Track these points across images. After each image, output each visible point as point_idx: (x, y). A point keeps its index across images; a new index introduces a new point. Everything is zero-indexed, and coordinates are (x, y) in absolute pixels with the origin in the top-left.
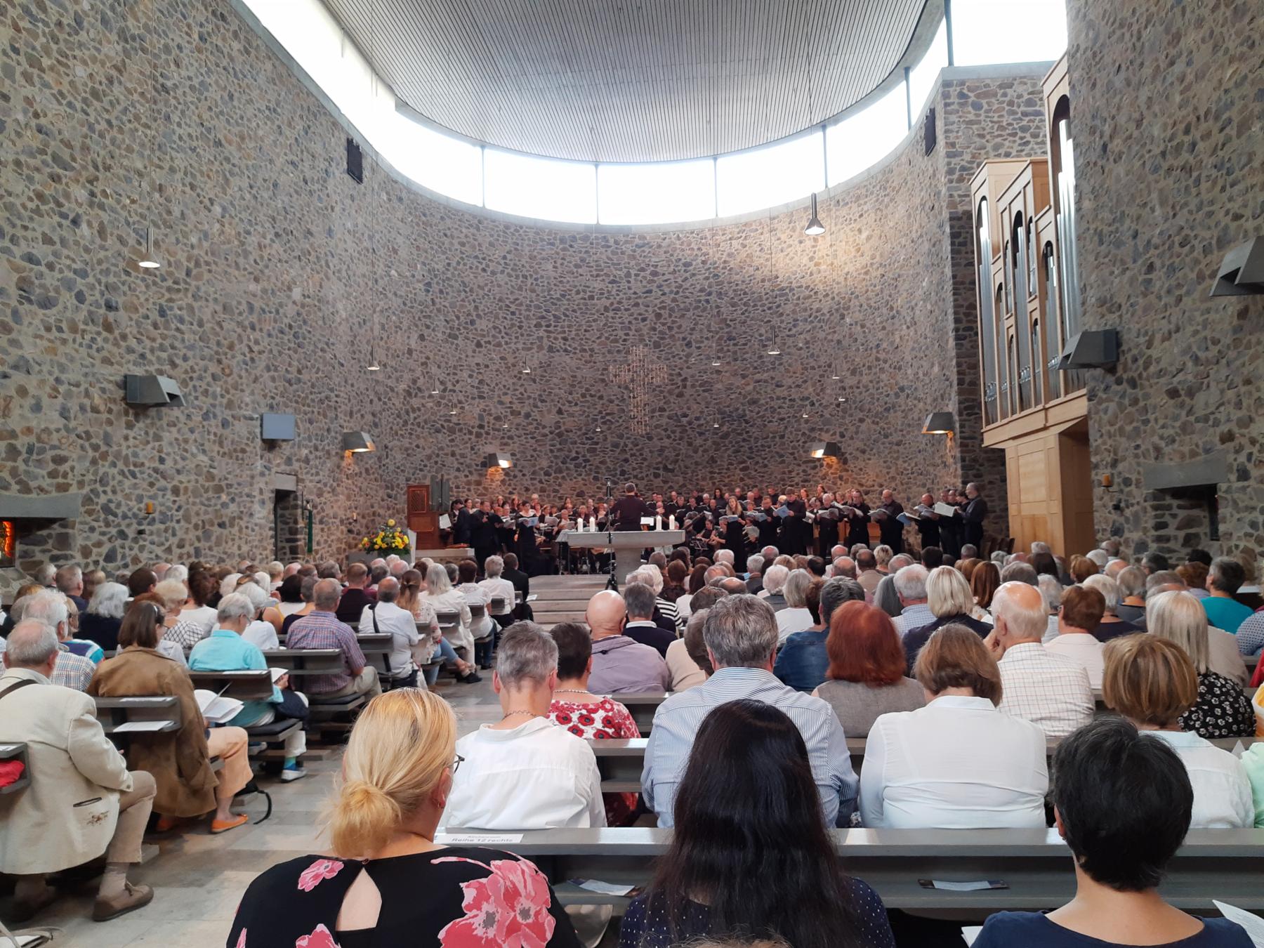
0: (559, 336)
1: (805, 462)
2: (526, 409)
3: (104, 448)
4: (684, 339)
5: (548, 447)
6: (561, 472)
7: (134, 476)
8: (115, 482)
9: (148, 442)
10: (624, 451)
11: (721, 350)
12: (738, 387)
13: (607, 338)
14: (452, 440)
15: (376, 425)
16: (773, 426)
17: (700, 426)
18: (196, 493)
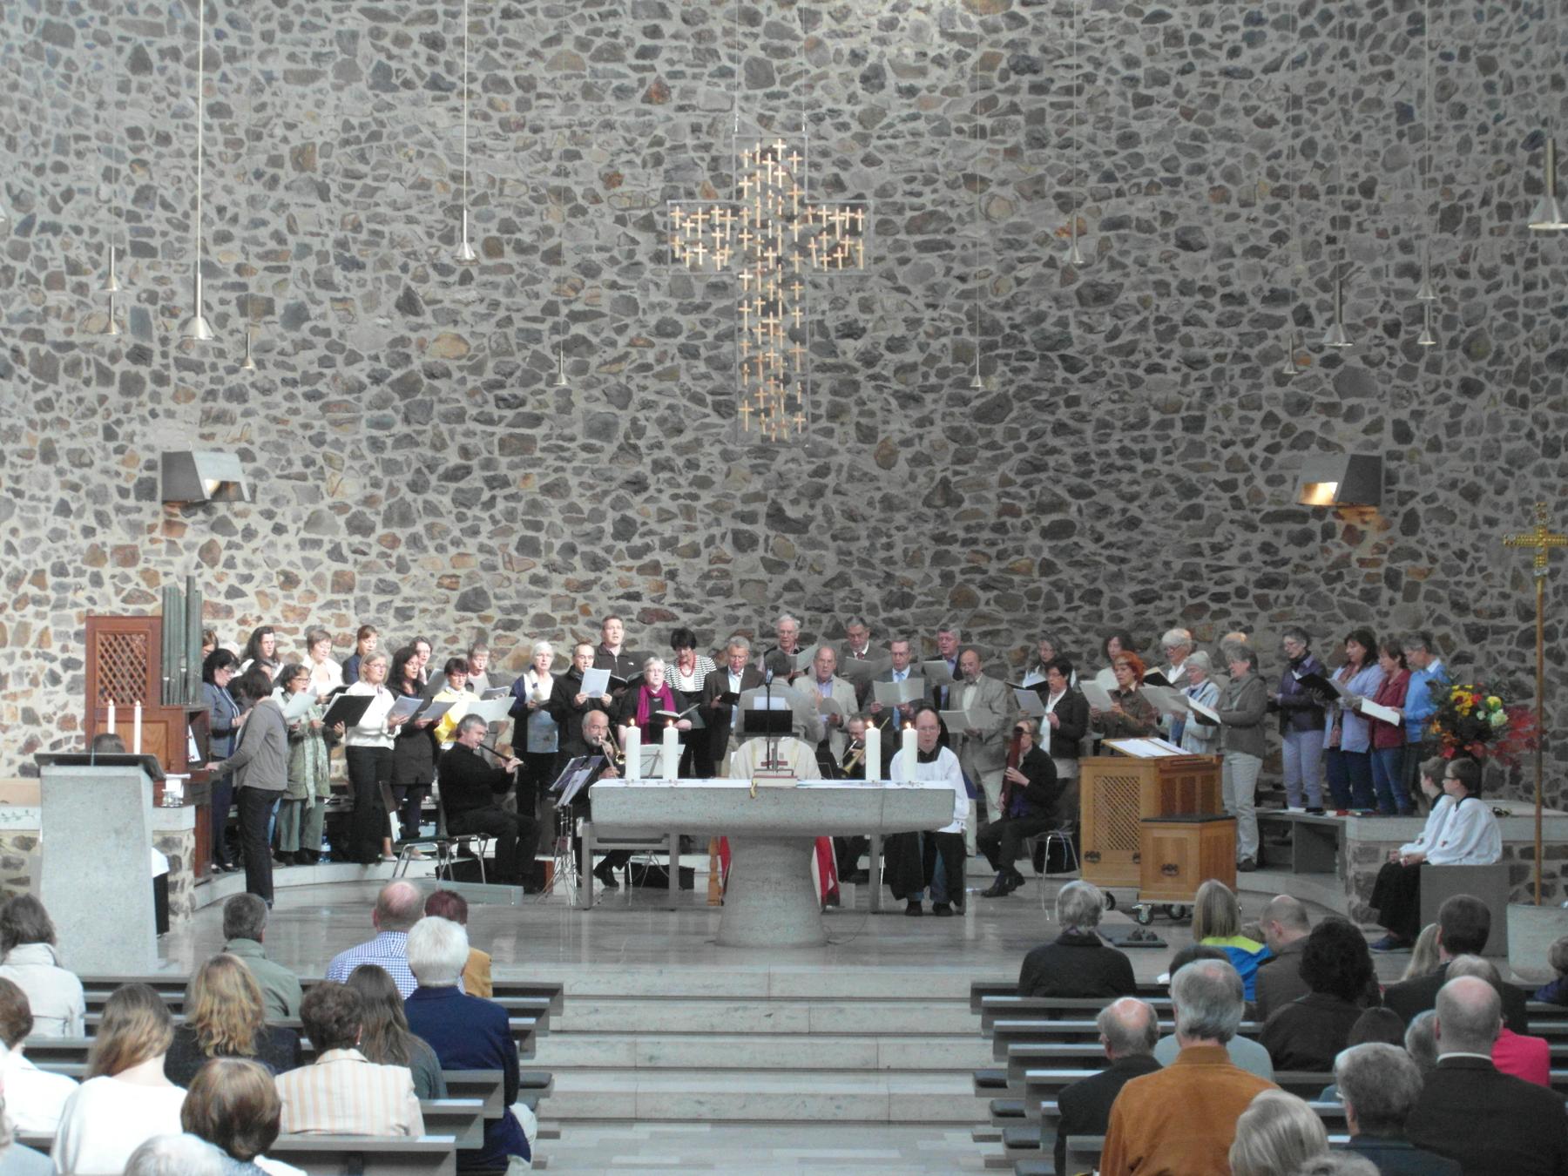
0: (414, 32)
1: (1270, 518)
2: (293, 293)
4: (857, 58)
5: (364, 431)
6: (405, 519)
10: (629, 450)
11: (989, 104)
12: (1044, 241)
13: (583, 44)
14: (46, 405)
16: (1166, 386)
17: (903, 370)
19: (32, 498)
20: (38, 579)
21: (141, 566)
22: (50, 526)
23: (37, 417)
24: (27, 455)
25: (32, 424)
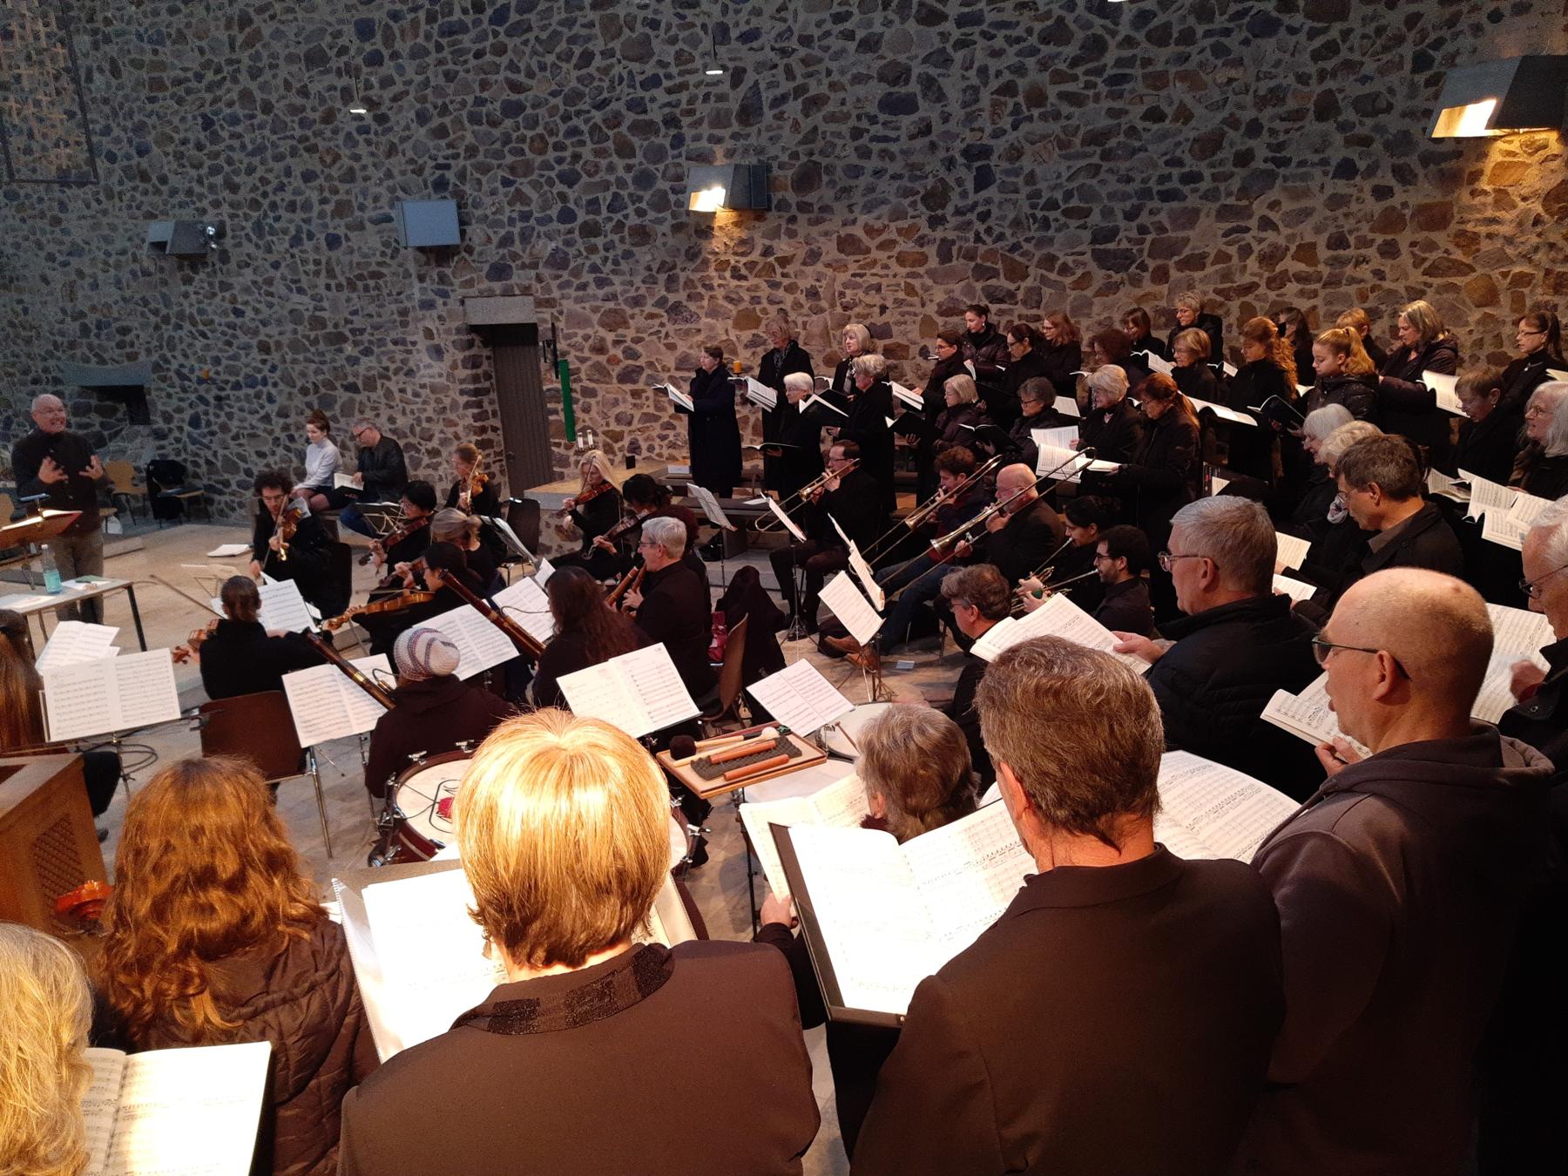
3: (164, 311)
7: (204, 335)
8: (184, 346)
9: (214, 295)
14: (1331, 49)
15: (897, 105)
18: (295, 346)
19: (1302, 164)
20: (1306, 252)
21: (1454, 227)
22: (1329, 191)
23: (1312, 69)
24: (1297, 115)
25: (1303, 79)
